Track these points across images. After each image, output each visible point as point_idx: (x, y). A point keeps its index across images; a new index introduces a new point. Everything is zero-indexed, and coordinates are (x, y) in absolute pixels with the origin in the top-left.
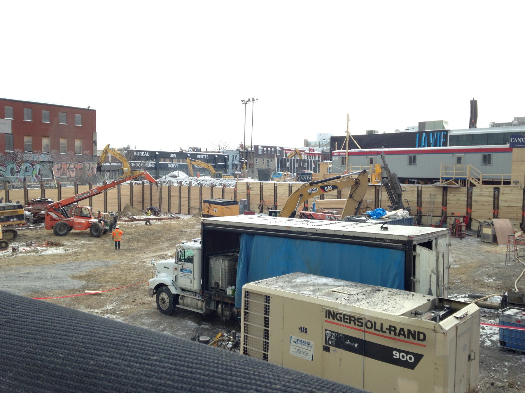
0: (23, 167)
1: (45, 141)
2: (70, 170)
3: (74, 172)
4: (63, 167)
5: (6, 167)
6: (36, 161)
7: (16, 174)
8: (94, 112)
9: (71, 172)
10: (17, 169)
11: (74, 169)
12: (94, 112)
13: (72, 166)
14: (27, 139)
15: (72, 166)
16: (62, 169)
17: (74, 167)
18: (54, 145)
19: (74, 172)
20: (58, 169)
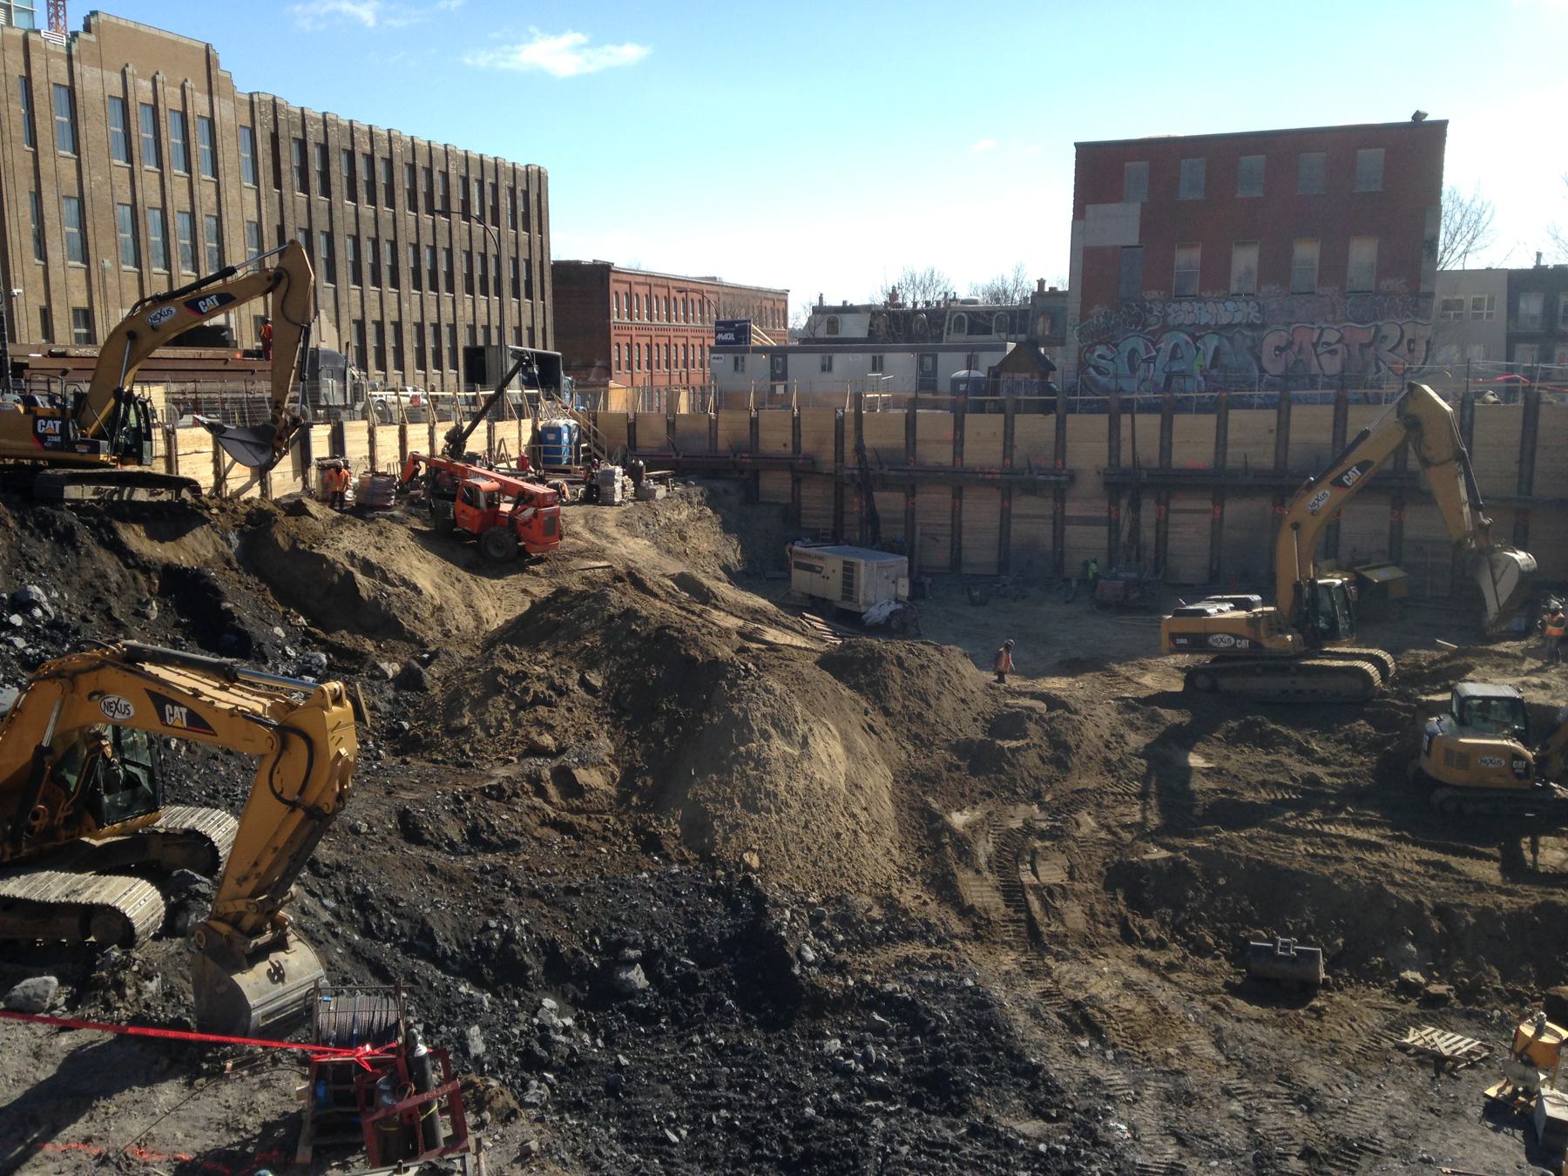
0: (1166, 345)
1: (1245, 259)
2: (1320, 350)
3: (1338, 359)
5: (1116, 346)
6: (1207, 326)
7: (1143, 366)
8: (1080, 147)
9: (1325, 359)
10: (1148, 351)
11: (1339, 347)
12: (1440, 128)
13: (1331, 336)
14: (1188, 258)
15: (1331, 336)
16: (1296, 348)
18: (1276, 269)
19: (1338, 359)
20: (1278, 348)
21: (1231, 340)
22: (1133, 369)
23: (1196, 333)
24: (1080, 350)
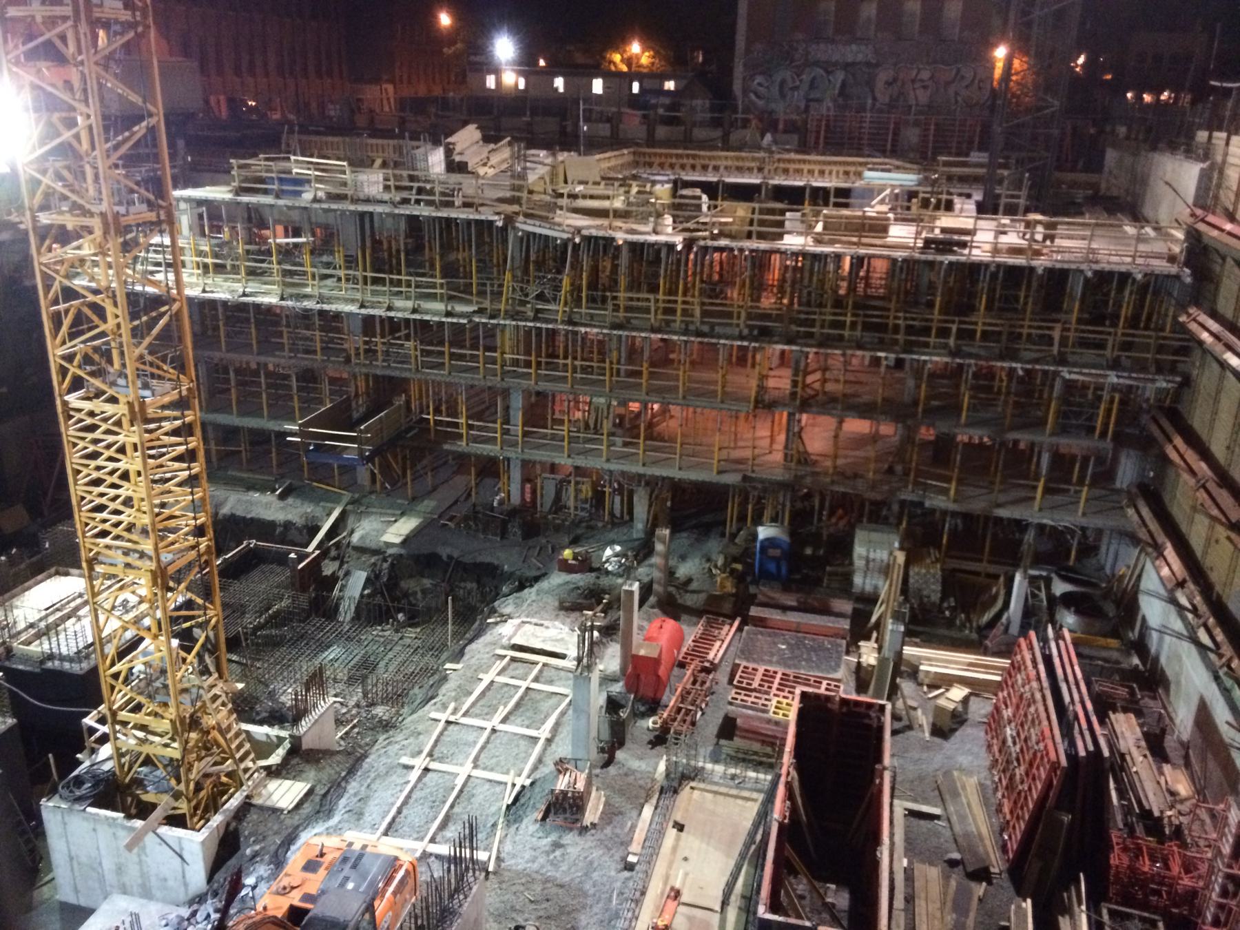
2: (917, 85)
4: (901, 76)
5: (771, 76)
6: (836, 64)
9: (920, 92)
10: (794, 82)
11: (930, 83)
15: (925, 75)
16: (899, 83)
17: (932, 78)
19: (929, 92)
21: (854, 75)
22: (783, 95)
23: (829, 67)
24: (744, 79)
